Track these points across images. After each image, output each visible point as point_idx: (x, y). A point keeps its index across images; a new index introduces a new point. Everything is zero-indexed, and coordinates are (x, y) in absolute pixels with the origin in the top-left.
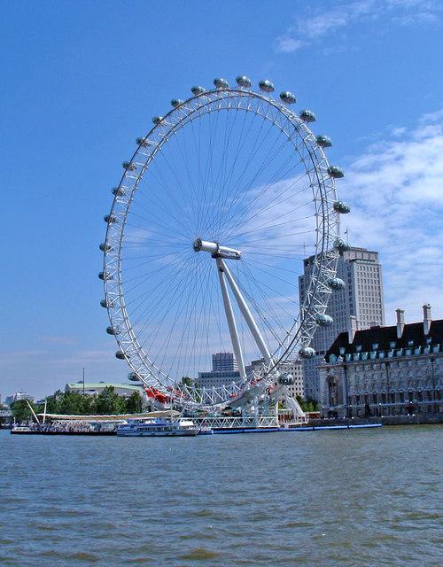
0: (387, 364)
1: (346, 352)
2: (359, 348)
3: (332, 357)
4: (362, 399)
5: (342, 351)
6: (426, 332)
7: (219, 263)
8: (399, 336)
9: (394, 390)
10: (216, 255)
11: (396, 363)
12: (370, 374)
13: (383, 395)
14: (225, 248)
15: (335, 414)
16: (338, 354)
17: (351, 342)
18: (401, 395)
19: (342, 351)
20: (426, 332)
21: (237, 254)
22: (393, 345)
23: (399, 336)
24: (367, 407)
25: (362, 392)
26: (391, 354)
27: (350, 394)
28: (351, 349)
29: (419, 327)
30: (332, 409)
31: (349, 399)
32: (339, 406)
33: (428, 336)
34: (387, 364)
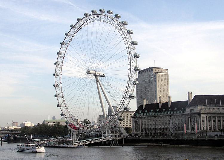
0: (155, 117)
1: (141, 112)
2: (146, 111)
3: (137, 115)
5: (140, 112)
7: (96, 78)
10: (95, 75)
12: (149, 121)
13: (154, 129)
14: (99, 73)
15: (136, 135)
17: (143, 109)
18: (160, 129)
19: (140, 112)
20: (169, 106)
21: (103, 75)
22: (158, 110)
24: (146, 133)
25: (146, 127)
26: (156, 114)
27: (143, 128)
28: (143, 111)
29: (167, 104)
30: (136, 133)
31: (142, 129)
32: (139, 132)
33: (170, 108)
34: (155, 117)
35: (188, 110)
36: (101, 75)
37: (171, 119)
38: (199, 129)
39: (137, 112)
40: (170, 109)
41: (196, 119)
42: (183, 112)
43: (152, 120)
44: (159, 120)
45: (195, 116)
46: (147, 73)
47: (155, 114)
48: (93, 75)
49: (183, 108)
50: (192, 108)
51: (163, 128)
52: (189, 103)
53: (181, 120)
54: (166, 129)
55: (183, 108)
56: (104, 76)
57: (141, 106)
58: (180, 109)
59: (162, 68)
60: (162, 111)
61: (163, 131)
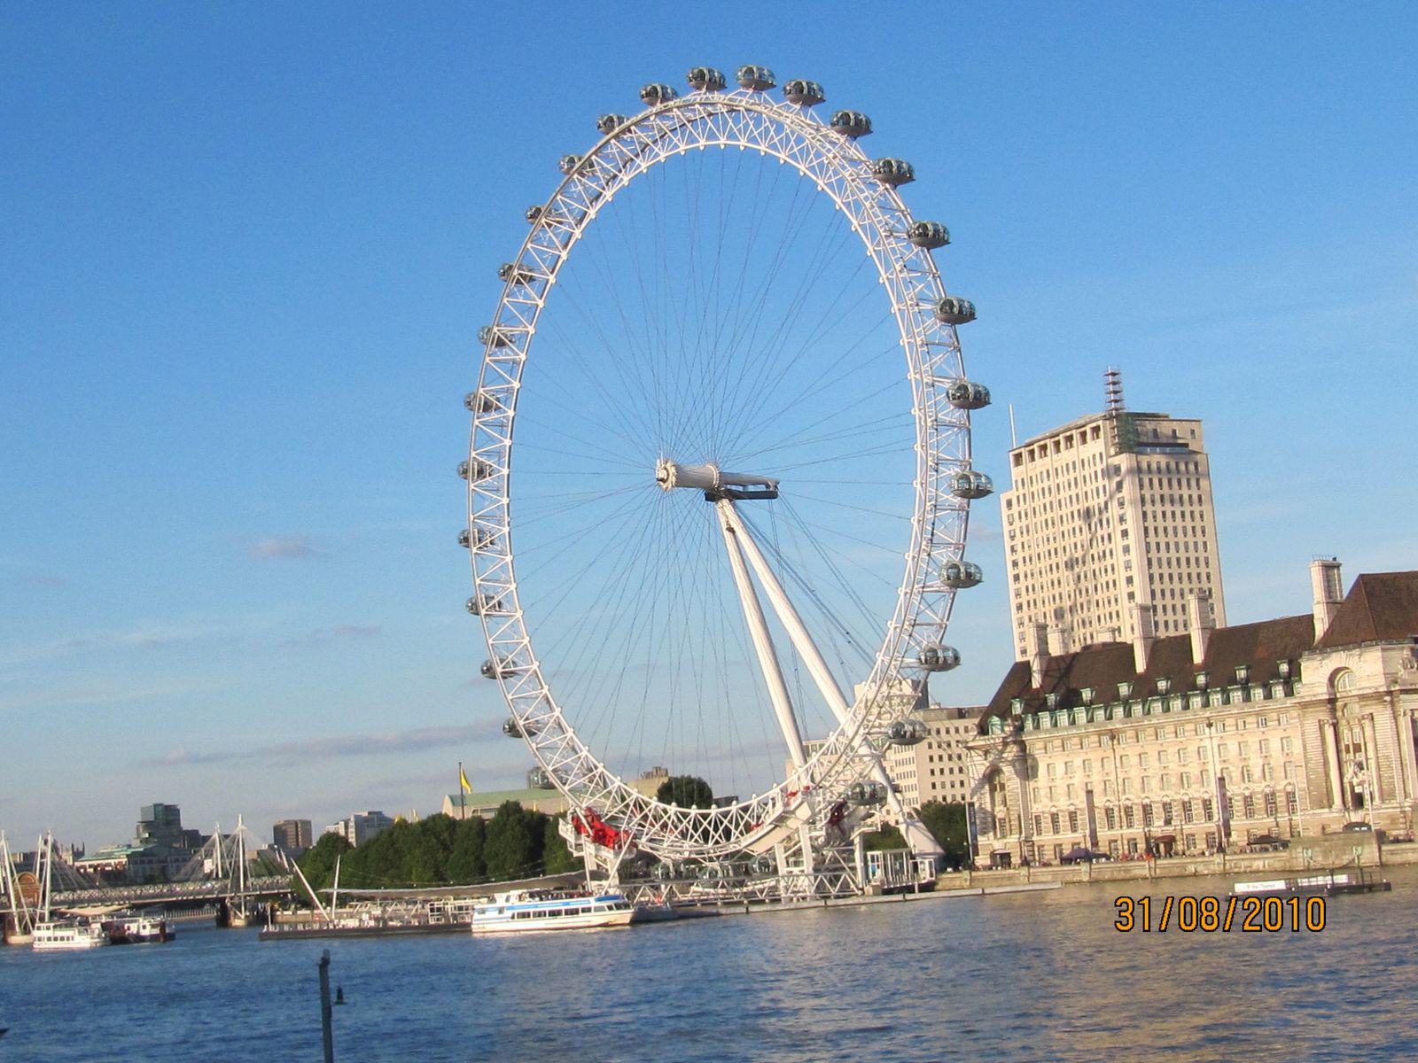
1: (1025, 712)
4: (1138, 814)
5: (1017, 708)
6: (1198, 657)
8: (1140, 666)
9: (1135, 797)
11: (1095, 738)
16: (1004, 713)
19: (1017, 708)
20: (1198, 657)
21: (768, 486)
23: (1140, 666)
27: (1036, 808)
28: (1036, 705)
33: (1206, 667)
34: (1113, 736)
35: (1314, 673)
36: (751, 488)
37: (1216, 742)
38: (1392, 795)
39: (1000, 707)
40: (1201, 680)
41: (1368, 733)
42: (1289, 693)
43: (1094, 756)
44: (1139, 750)
45: (1367, 711)
46: (1067, 456)
47: (1110, 718)
48: (701, 494)
49: (1284, 668)
50: (1337, 659)
51: (1167, 807)
52: (1320, 628)
53: (1275, 745)
54: (1186, 806)
55: (1284, 668)
56: (771, 495)
57: (1022, 670)
58: (1264, 676)
59: (1165, 418)
60: (1154, 691)
61: (1168, 822)
